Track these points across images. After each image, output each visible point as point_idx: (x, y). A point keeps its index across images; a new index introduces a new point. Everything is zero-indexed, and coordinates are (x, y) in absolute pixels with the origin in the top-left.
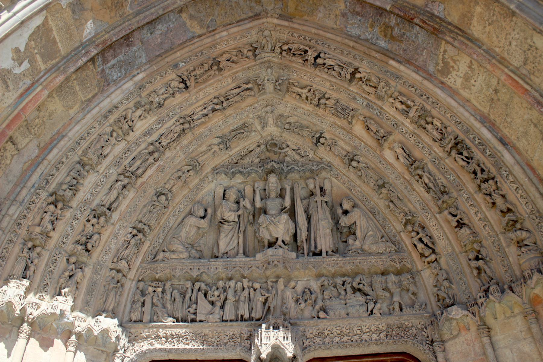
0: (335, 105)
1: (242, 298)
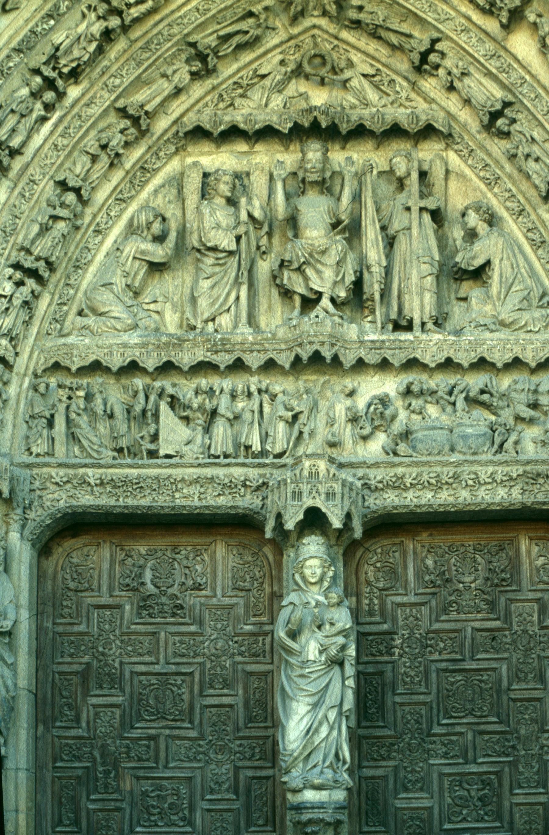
1: (247, 416)
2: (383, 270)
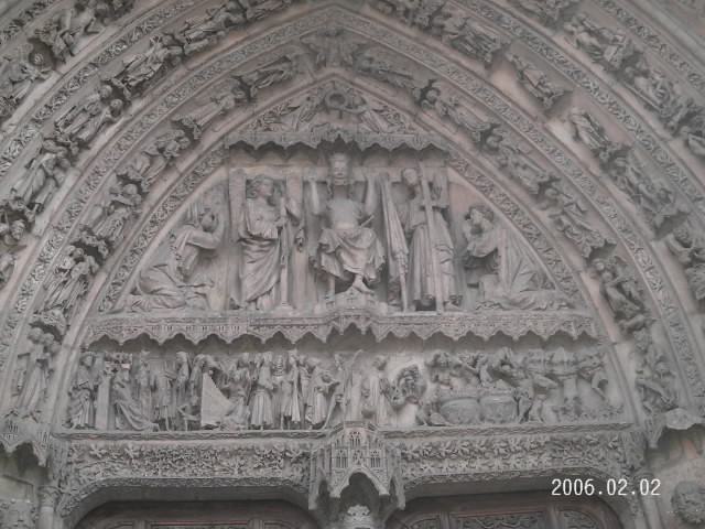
0: (462, 28)
1: (287, 387)
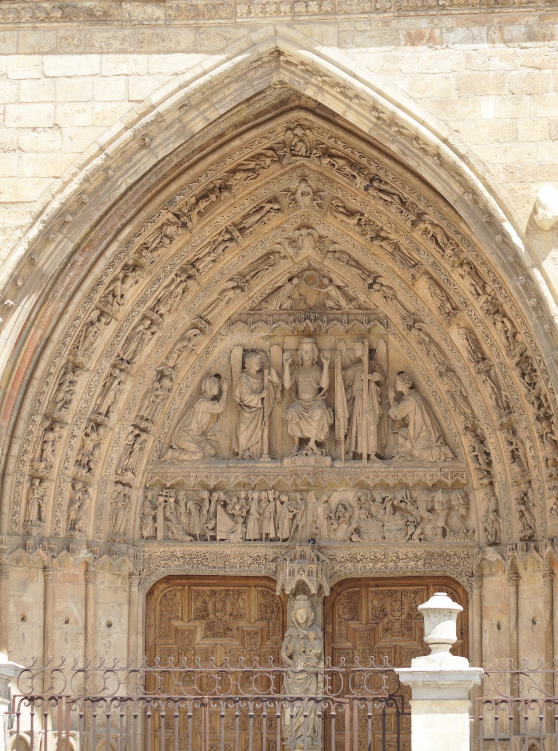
1: (267, 514)
2: (346, 420)
